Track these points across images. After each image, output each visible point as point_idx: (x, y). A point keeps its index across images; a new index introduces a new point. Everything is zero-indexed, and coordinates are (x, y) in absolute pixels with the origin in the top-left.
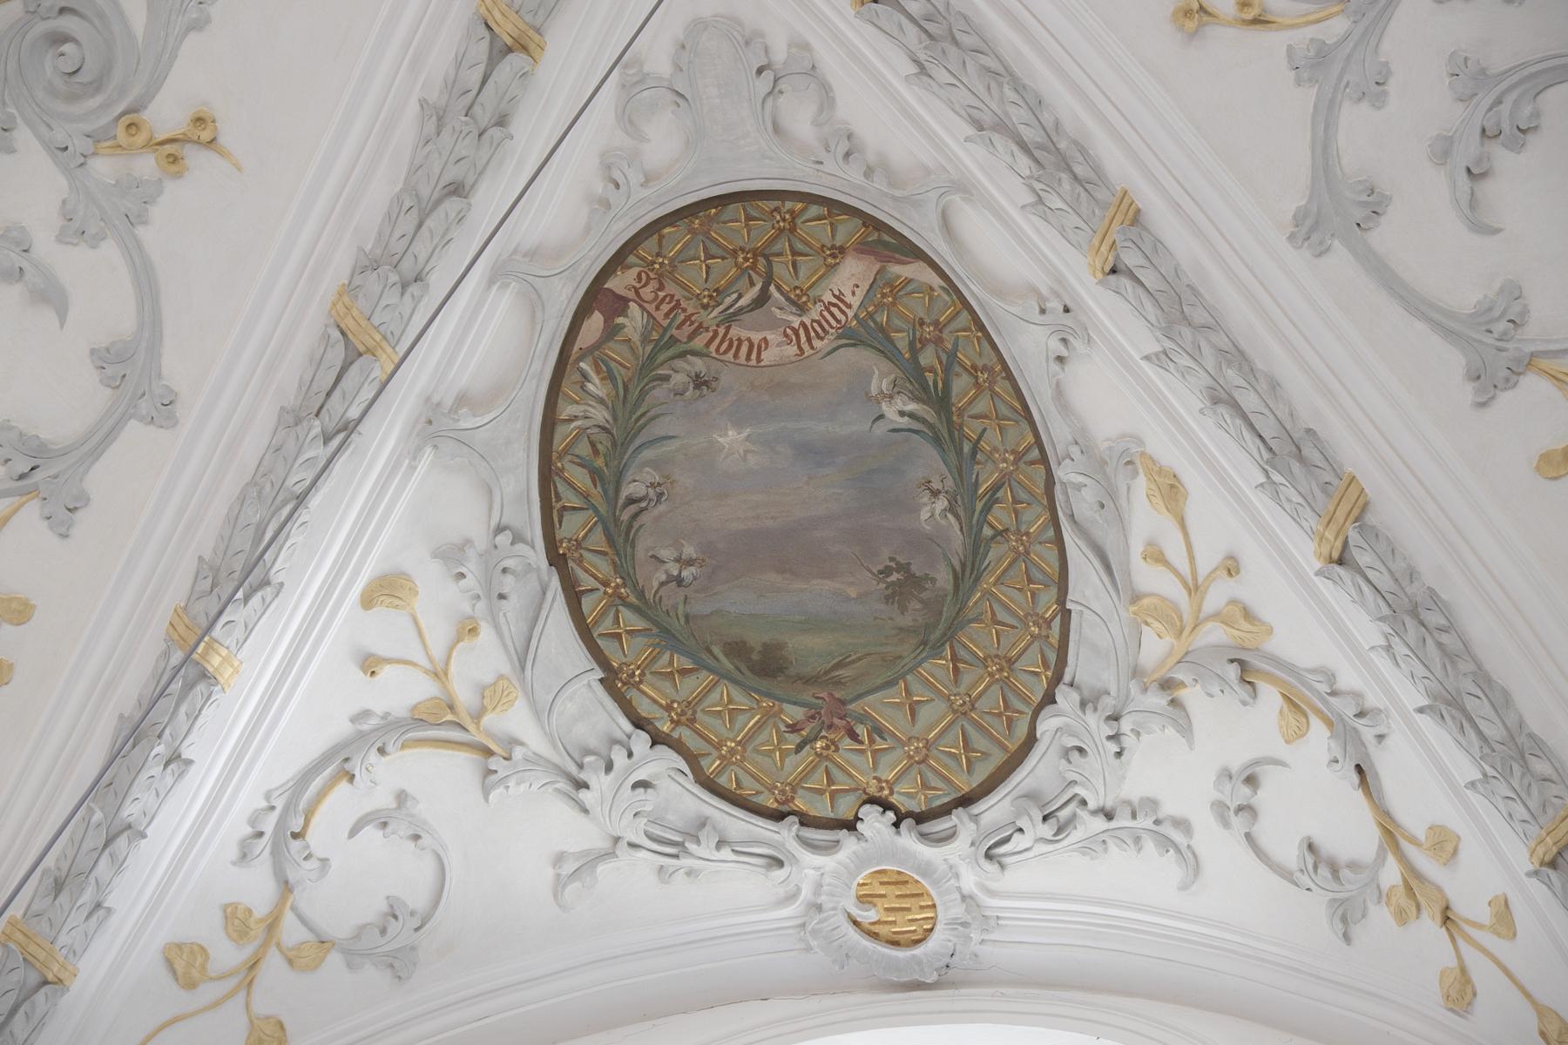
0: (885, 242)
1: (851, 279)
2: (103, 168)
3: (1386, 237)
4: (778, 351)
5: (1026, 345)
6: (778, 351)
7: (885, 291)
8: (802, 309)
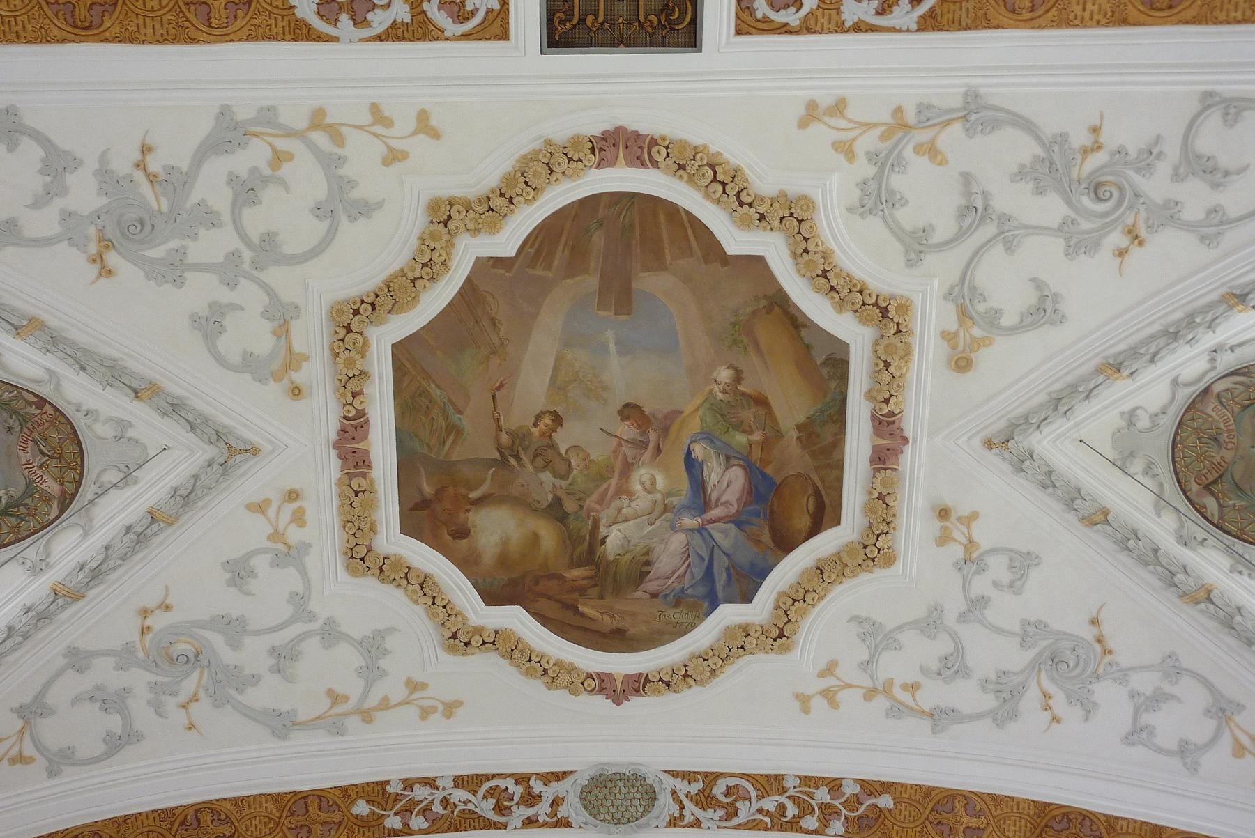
0: (66, 500)
1: (52, 486)
2: (92, 231)
3: (71, 675)
4: (24, 457)
5: (30, 550)
6: (24, 457)
7: (48, 499)
8: (40, 467)
